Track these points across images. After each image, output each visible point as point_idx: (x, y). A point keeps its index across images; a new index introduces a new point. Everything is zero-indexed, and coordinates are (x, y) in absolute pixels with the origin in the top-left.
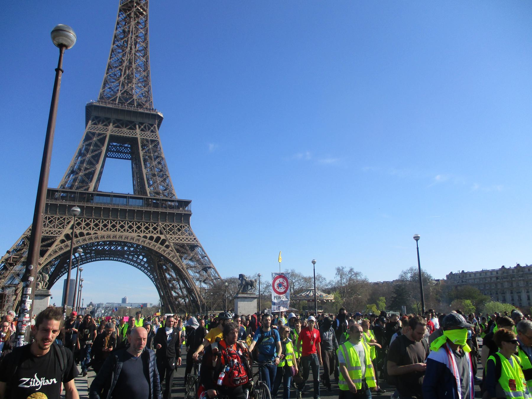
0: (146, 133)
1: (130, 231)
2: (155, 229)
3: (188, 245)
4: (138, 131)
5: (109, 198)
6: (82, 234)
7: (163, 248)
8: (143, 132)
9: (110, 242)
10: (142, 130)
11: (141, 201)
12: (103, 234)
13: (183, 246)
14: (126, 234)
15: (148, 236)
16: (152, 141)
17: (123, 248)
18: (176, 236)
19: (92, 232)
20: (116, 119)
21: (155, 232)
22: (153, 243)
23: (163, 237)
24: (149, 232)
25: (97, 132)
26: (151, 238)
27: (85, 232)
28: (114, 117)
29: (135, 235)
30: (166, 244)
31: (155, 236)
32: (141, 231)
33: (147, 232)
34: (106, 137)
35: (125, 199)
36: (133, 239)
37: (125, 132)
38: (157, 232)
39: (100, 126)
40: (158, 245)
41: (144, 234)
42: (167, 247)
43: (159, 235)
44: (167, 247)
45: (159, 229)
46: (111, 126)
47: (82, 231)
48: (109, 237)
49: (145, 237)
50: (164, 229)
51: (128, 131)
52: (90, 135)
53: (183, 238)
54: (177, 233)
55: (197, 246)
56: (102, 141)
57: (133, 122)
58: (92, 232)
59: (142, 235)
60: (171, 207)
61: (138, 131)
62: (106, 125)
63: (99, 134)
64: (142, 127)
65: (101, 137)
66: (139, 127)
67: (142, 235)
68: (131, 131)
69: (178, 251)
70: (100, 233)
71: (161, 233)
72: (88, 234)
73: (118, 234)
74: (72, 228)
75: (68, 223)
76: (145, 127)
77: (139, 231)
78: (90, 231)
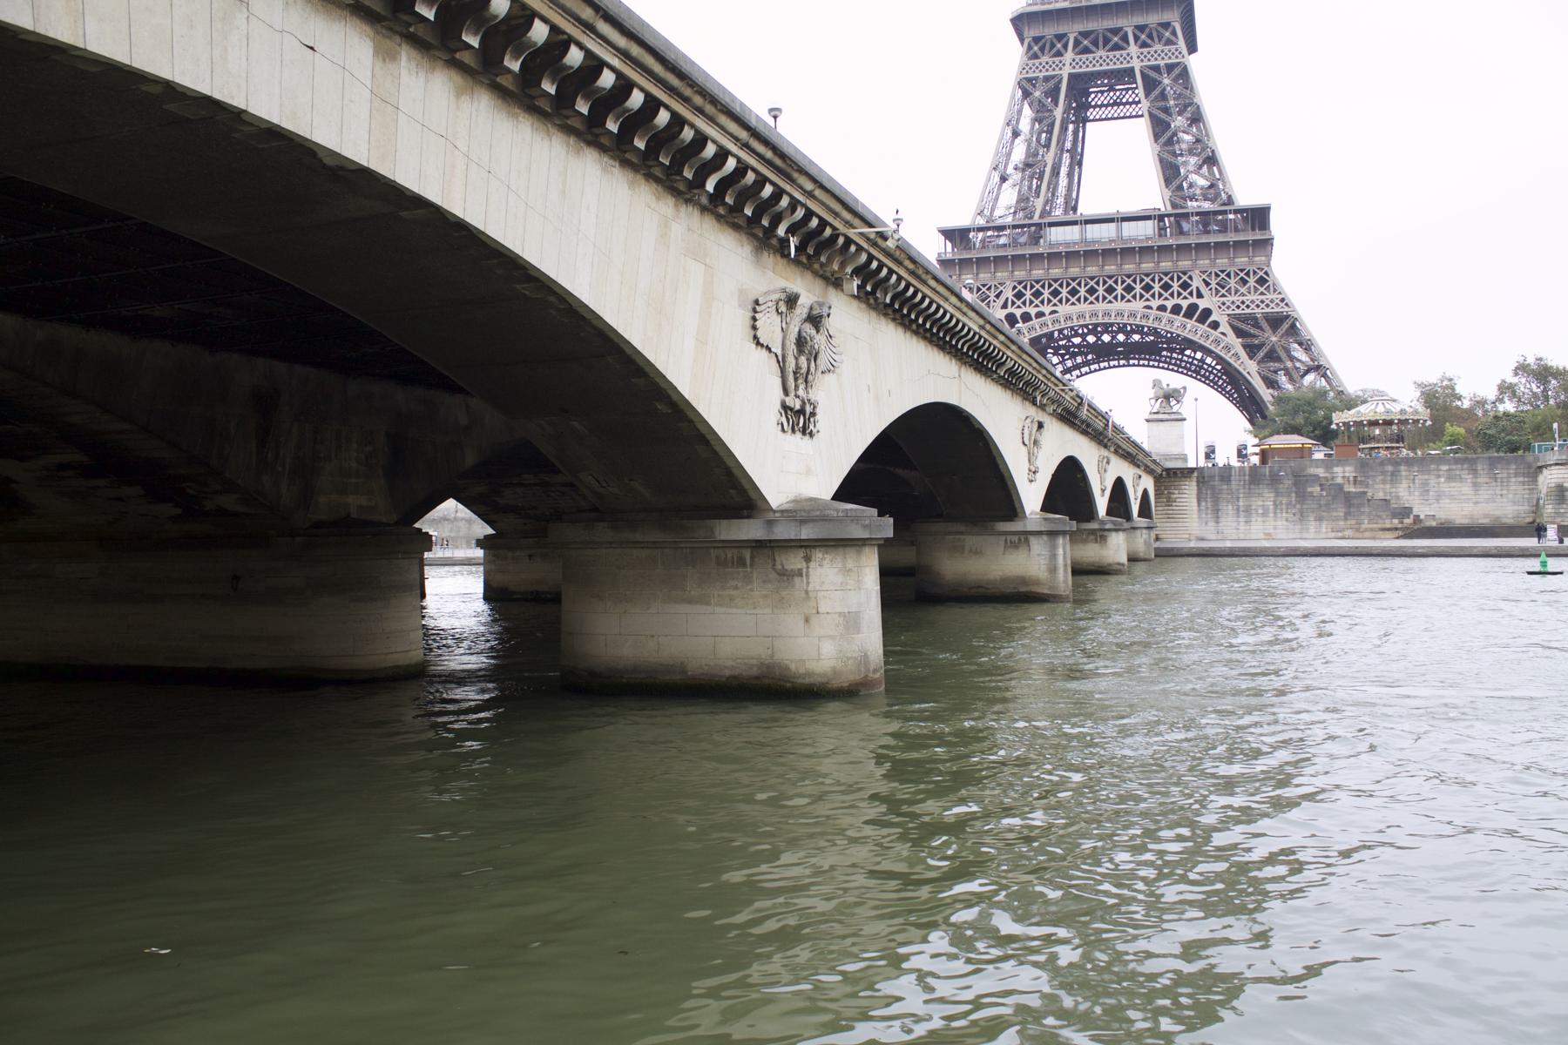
0: (1152, 50)
1: (1129, 297)
2: (1185, 286)
3: (1267, 317)
4: (1133, 49)
5: (1076, 228)
6: (1026, 317)
7: (1205, 327)
8: (1145, 50)
9: (1096, 325)
10: (1144, 45)
11: (1150, 223)
12: (1070, 313)
13: (1252, 320)
14: (1119, 305)
15: (1169, 304)
16: (1170, 68)
17: (1114, 338)
18: (1235, 298)
19: (1047, 309)
20: (1081, 33)
21: (1185, 294)
22: (1179, 319)
23: (1203, 304)
24: (1172, 295)
25: (1041, 75)
26: (1176, 310)
27: (1033, 311)
28: (1073, 29)
29: (1137, 305)
30: (1212, 318)
31: (1185, 304)
32: (1153, 296)
33: (1166, 295)
34: (1060, 82)
35: (1113, 225)
36: (1133, 315)
37: (1102, 60)
38: (1191, 294)
39: (1044, 59)
40: (1191, 323)
41: (1161, 302)
42: (1215, 325)
43: (1194, 300)
44: (1215, 325)
45: (1196, 283)
46: (1069, 55)
47: (1028, 309)
48: (1081, 316)
49: (1162, 308)
50: (1207, 284)
51: (1111, 54)
52: (1028, 87)
53: (1254, 302)
54: (1237, 291)
55: (1288, 317)
56: (1054, 94)
57: (1120, 29)
58: (1047, 309)
59: (1155, 303)
60: (1224, 228)
61: (1133, 49)
62: (1059, 54)
63: (1047, 79)
64: (1143, 37)
65: (1051, 84)
66: (1136, 38)
67: (1155, 303)
68: (1117, 53)
69: (1239, 333)
70: (1064, 309)
71: (1200, 295)
72: (1040, 315)
73: (1101, 307)
74: (1005, 306)
75: (997, 296)
76: (1150, 36)
77: (1147, 296)
78: (1042, 309)
